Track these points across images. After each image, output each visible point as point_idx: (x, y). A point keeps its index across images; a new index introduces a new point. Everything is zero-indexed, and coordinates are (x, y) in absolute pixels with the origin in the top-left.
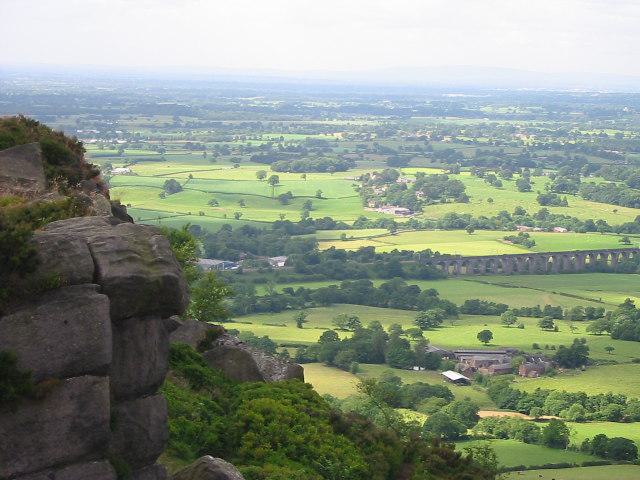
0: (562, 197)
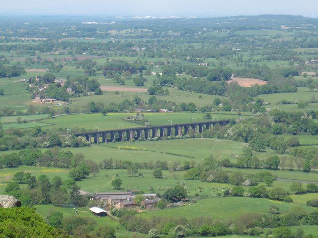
0: (164, 88)
